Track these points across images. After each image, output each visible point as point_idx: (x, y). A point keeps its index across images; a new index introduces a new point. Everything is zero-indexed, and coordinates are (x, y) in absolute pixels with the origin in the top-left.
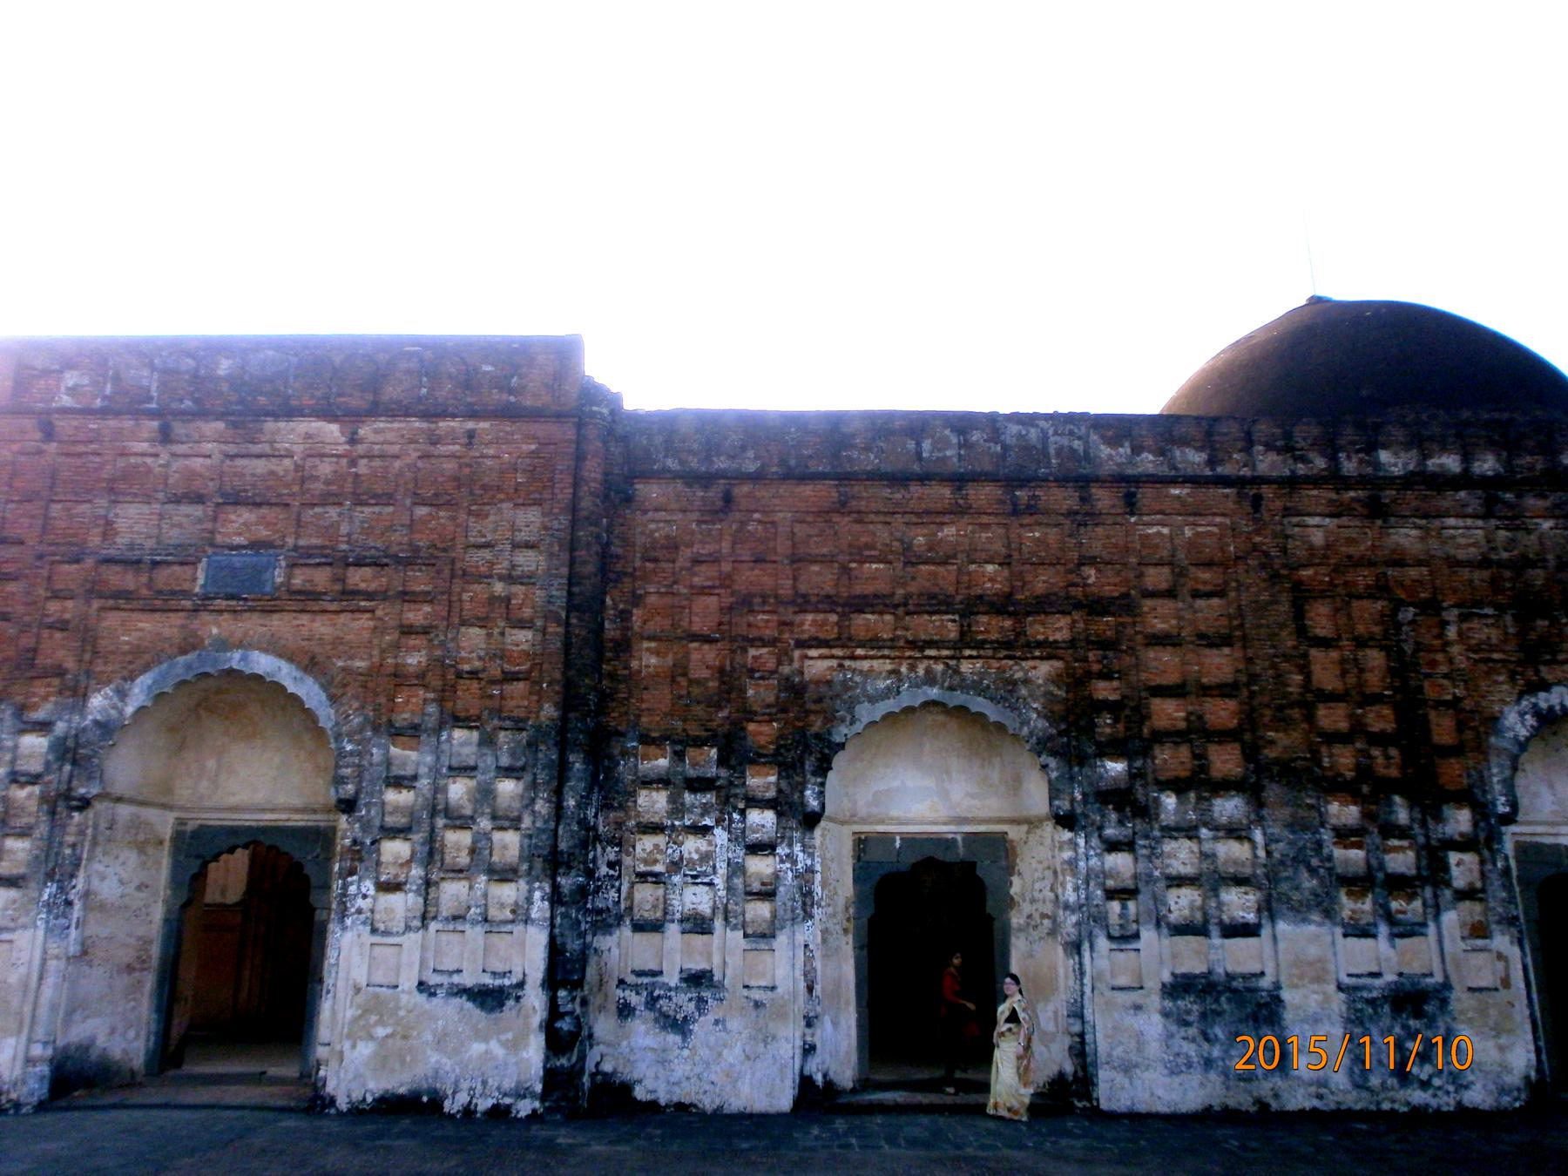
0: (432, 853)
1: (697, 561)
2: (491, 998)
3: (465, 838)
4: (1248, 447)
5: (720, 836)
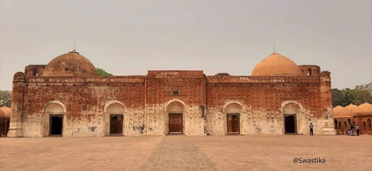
4: (262, 80)
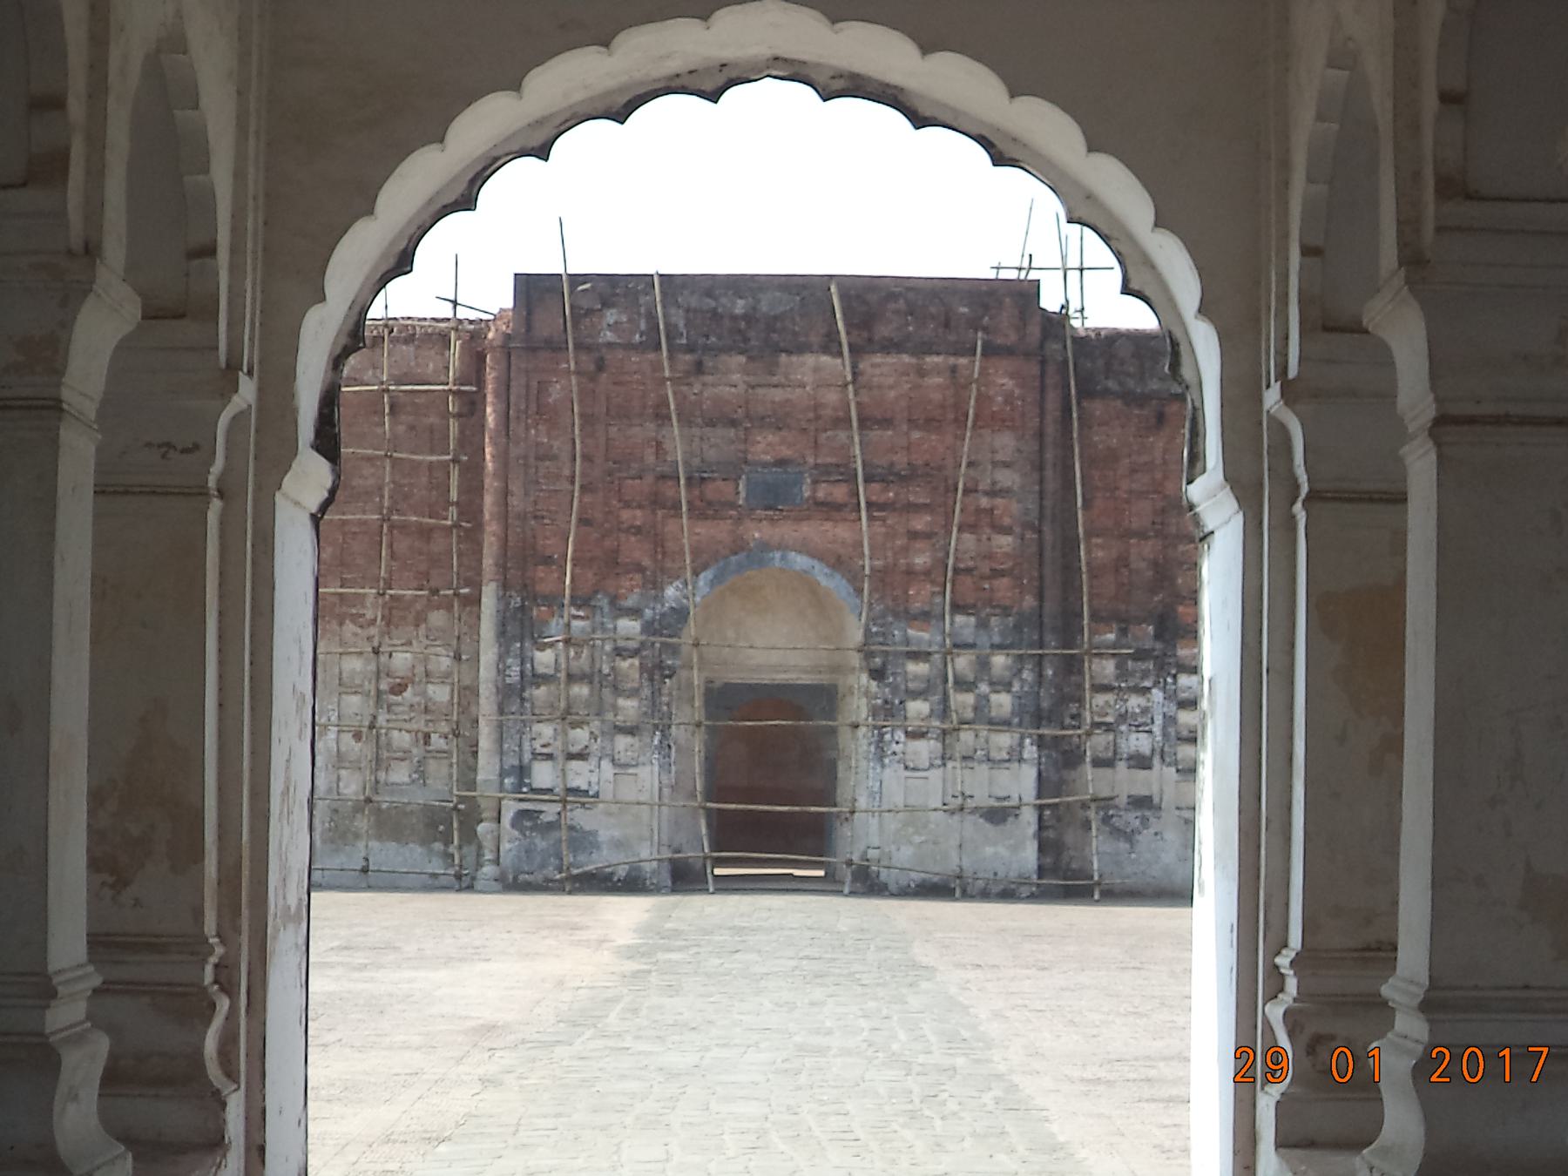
0: (944, 711)
1: (1133, 471)
2: (998, 815)
3: (969, 699)
5: (1157, 695)
